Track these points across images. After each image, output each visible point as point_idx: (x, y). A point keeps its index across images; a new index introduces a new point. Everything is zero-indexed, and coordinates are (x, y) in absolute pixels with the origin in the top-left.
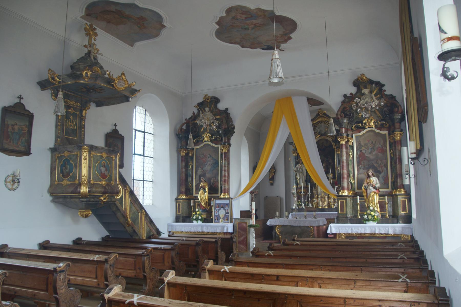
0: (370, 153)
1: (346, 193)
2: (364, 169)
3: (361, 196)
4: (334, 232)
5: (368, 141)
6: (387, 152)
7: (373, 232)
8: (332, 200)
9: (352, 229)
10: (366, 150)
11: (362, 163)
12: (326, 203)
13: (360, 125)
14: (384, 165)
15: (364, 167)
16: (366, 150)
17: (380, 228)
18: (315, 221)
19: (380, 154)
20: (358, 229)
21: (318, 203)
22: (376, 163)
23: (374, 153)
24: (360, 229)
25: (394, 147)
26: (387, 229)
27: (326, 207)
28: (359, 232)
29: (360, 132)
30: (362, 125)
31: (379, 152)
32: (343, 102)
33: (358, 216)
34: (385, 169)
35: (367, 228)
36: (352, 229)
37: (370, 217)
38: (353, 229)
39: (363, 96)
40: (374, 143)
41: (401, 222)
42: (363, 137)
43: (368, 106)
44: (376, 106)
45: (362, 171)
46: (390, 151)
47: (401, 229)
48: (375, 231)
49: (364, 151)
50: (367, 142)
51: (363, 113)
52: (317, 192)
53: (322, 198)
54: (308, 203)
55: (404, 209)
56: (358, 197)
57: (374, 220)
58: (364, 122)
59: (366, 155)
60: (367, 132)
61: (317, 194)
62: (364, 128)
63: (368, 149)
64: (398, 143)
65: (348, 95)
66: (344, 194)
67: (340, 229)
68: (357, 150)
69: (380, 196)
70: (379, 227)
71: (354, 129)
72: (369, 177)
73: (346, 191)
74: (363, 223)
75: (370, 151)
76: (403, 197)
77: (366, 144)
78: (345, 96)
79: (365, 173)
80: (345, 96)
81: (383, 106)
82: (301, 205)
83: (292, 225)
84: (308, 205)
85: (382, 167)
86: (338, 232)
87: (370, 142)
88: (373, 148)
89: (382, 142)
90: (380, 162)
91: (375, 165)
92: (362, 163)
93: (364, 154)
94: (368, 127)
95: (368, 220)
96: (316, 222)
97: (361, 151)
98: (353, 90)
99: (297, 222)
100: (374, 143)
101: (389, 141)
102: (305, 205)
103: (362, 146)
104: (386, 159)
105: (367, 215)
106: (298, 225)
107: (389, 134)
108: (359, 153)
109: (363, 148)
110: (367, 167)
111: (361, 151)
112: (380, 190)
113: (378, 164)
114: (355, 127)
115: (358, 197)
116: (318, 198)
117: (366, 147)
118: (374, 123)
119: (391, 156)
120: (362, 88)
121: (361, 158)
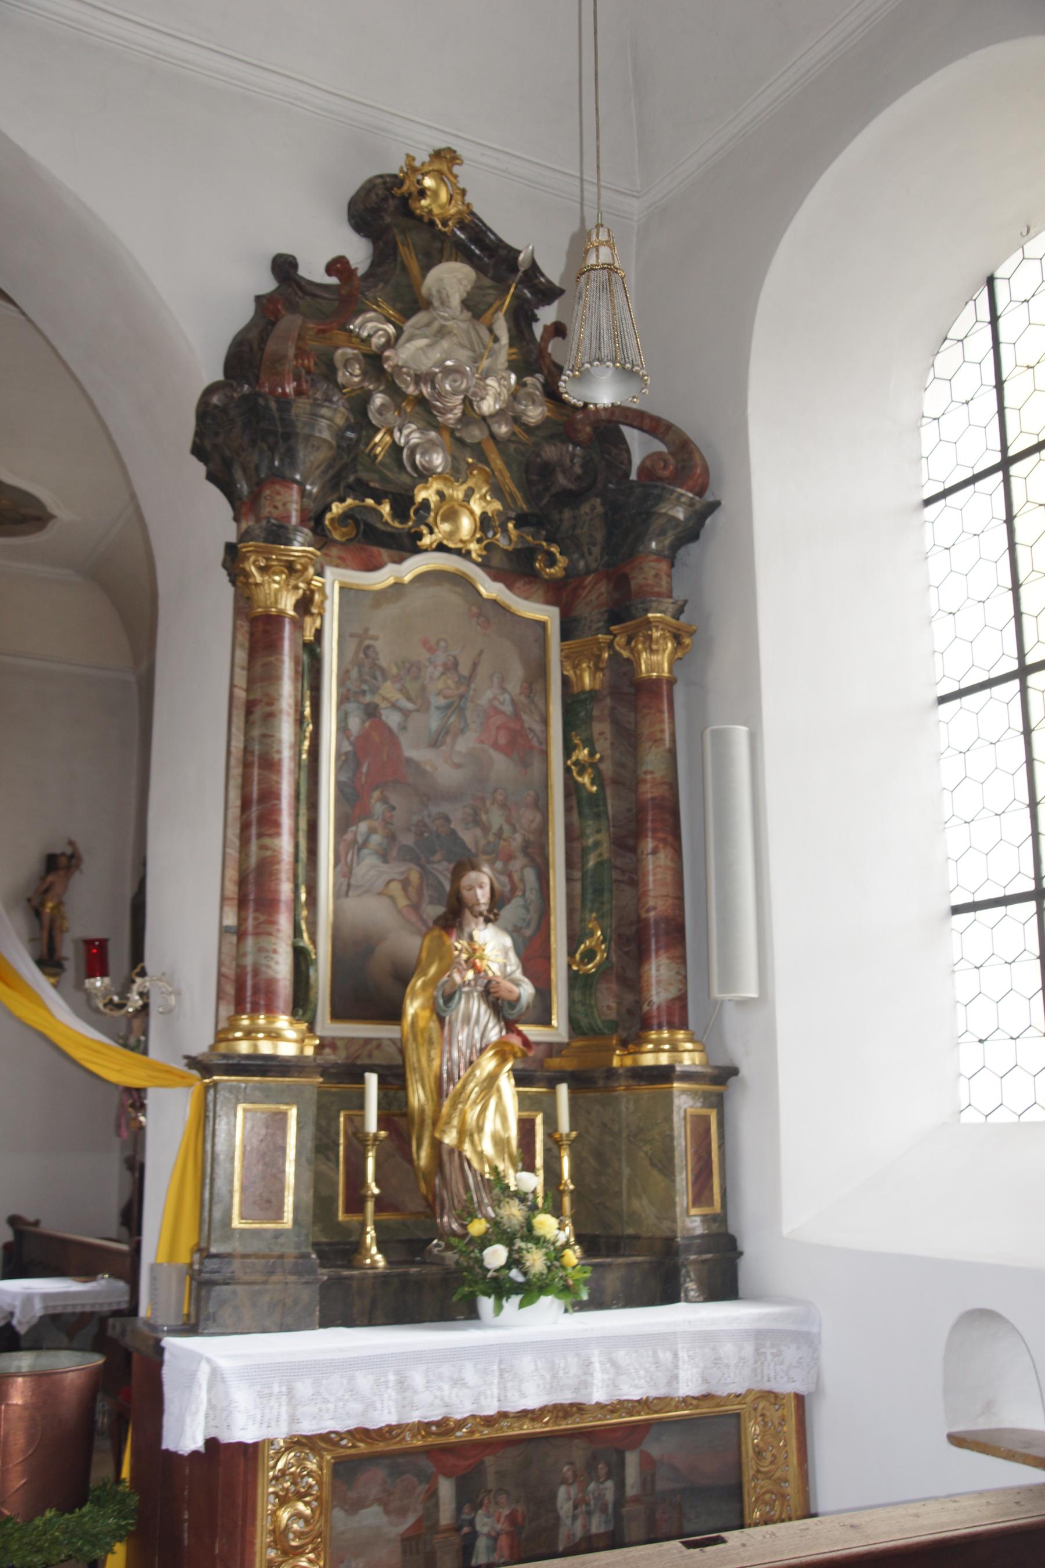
0: (435, 743)
1: (287, 1038)
2: (384, 857)
3: (394, 1080)
4: (244, 1430)
5: (431, 650)
6: (545, 754)
7: (566, 1397)
9: (402, 1385)
10: (406, 714)
11: (378, 808)
13: (386, 509)
14: (526, 847)
15: (392, 837)
16: (406, 714)
17: (622, 1356)
19: (501, 765)
20: (458, 1382)
22: (475, 820)
23: (464, 744)
24: (470, 1375)
25: (601, 728)
26: (665, 1356)
28: (462, 1407)
29: (373, 566)
30: (401, 511)
31: (495, 745)
32: (267, 308)
33: (357, 1247)
34: (530, 875)
35: (526, 1364)
36: (402, 1385)
37: (536, 1260)
38: (417, 1379)
39: (420, 318)
40: (464, 669)
41: (691, 1286)
42: (390, 610)
43: (455, 392)
44: (499, 414)
45: (368, 866)
46: (568, 749)
47: (749, 1349)
48: (585, 1384)
49: (392, 719)
50: (424, 655)
51: (411, 435)
55: (701, 1192)
56: (372, 1080)
57: (566, 1290)
58: (421, 495)
59: (409, 752)
60: (422, 578)
62: (407, 545)
63: (424, 707)
64: (658, 695)
65: (313, 269)
66: (266, 1048)
67: (304, 1388)
68: (343, 700)
69: (521, 1079)
70: (610, 1342)
71: (336, 536)
72: (454, 915)
73: (282, 1022)
74: (470, 1313)
75: (434, 722)
76: (693, 1094)
77: (412, 669)
78: (284, 267)
79: (395, 888)
80: (284, 267)
81: (528, 429)
85: (509, 857)
86: (280, 1433)
87: (441, 657)
88: (456, 706)
89: (517, 673)
90: (496, 818)
91: (468, 837)
92: (378, 808)
93: (391, 738)
94: (441, 548)
95: (530, 1290)
97: (371, 712)
98: (358, 252)
100: (464, 669)
101: (565, 681)
103: (385, 678)
104: (542, 805)
105: (500, 1233)
107: (567, 633)
108: (355, 724)
109: (389, 690)
110: (408, 840)
111: (371, 712)
112: (533, 1032)
113: (485, 829)
114: (345, 518)
115: (372, 1080)
117: (412, 687)
118: (484, 523)
119: (572, 789)
120: (414, 266)
121: (373, 762)
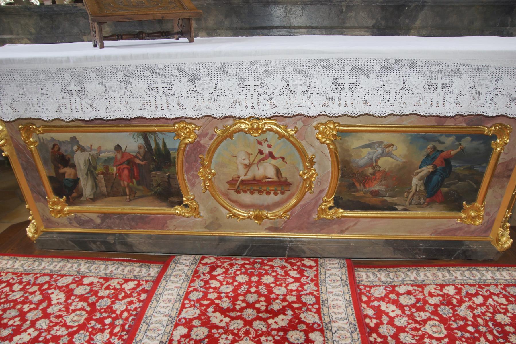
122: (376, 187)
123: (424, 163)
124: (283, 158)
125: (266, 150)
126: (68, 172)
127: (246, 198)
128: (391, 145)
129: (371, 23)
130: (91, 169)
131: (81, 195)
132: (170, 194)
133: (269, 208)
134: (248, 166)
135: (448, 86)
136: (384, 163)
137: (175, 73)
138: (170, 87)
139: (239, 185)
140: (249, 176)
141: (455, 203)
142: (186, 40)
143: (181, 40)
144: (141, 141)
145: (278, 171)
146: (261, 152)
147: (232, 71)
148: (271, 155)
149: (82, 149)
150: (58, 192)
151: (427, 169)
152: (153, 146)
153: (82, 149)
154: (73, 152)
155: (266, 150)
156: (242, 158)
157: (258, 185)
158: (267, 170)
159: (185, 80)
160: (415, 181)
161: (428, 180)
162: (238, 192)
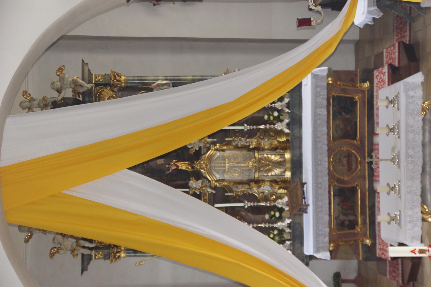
8: (266, 143)
12: (275, 158)
18: (407, 97)
21: (274, 182)
27: (288, 156)
52: (241, 183)
53: (258, 169)
54: (274, 208)
61: (248, 182)
82: (281, 232)
83: (420, 169)
84: (281, 210)
96: (411, 93)
99: (411, 152)
102: (281, 219)
106: (419, 149)
116: (258, 182)
122: (349, 128)
123: (342, 115)
124: (341, 156)
125: (338, 160)
126: (347, 223)
127: (354, 166)
128: (336, 125)
129: (298, 128)
130: (345, 215)
131: (354, 220)
132: (353, 190)
133: (357, 159)
134: (343, 166)
135: (320, 115)
136: (342, 126)
137: (317, 182)
138: (320, 183)
139: (350, 169)
140: (347, 166)
141: (354, 103)
142: (305, 186)
143: (305, 189)
144: (336, 197)
145: (345, 157)
146: (339, 162)
147: (317, 167)
148: (340, 159)
149: (339, 216)
150: (354, 228)
151: (343, 114)
152: (337, 193)
153: (339, 216)
154: (340, 219)
155: (338, 160)
156: (341, 167)
157: (349, 163)
158: (345, 161)
159: (319, 179)
160: (347, 117)
161: (347, 113)
162: (351, 169)
